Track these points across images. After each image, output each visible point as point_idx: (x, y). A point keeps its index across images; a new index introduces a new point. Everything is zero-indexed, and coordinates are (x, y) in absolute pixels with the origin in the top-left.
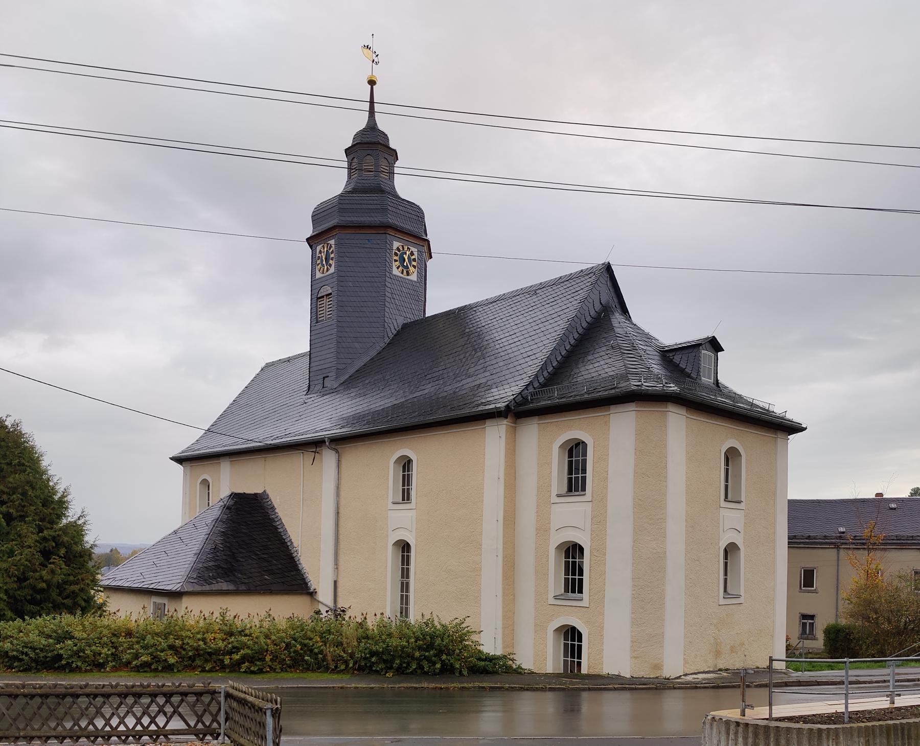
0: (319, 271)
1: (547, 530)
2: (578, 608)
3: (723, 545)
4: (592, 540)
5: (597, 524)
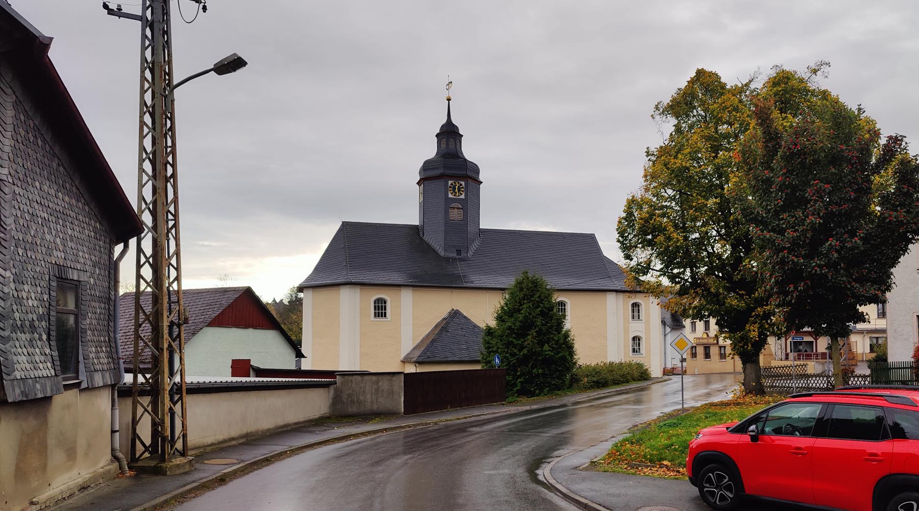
0: (452, 194)
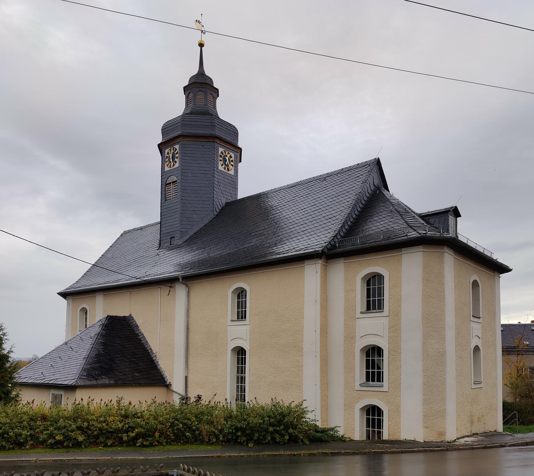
0: (167, 166)
1: (353, 338)
2: (380, 392)
3: (473, 346)
4: (389, 343)
5: (393, 332)
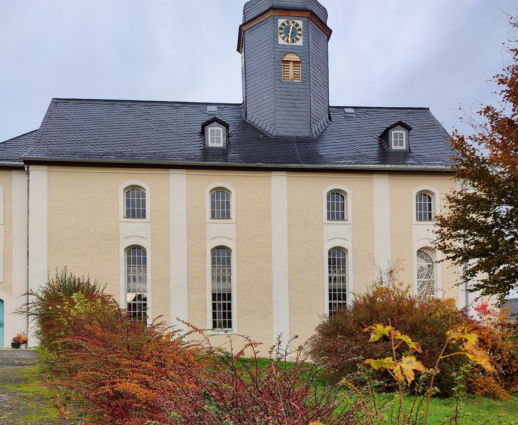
0: (283, 38)
